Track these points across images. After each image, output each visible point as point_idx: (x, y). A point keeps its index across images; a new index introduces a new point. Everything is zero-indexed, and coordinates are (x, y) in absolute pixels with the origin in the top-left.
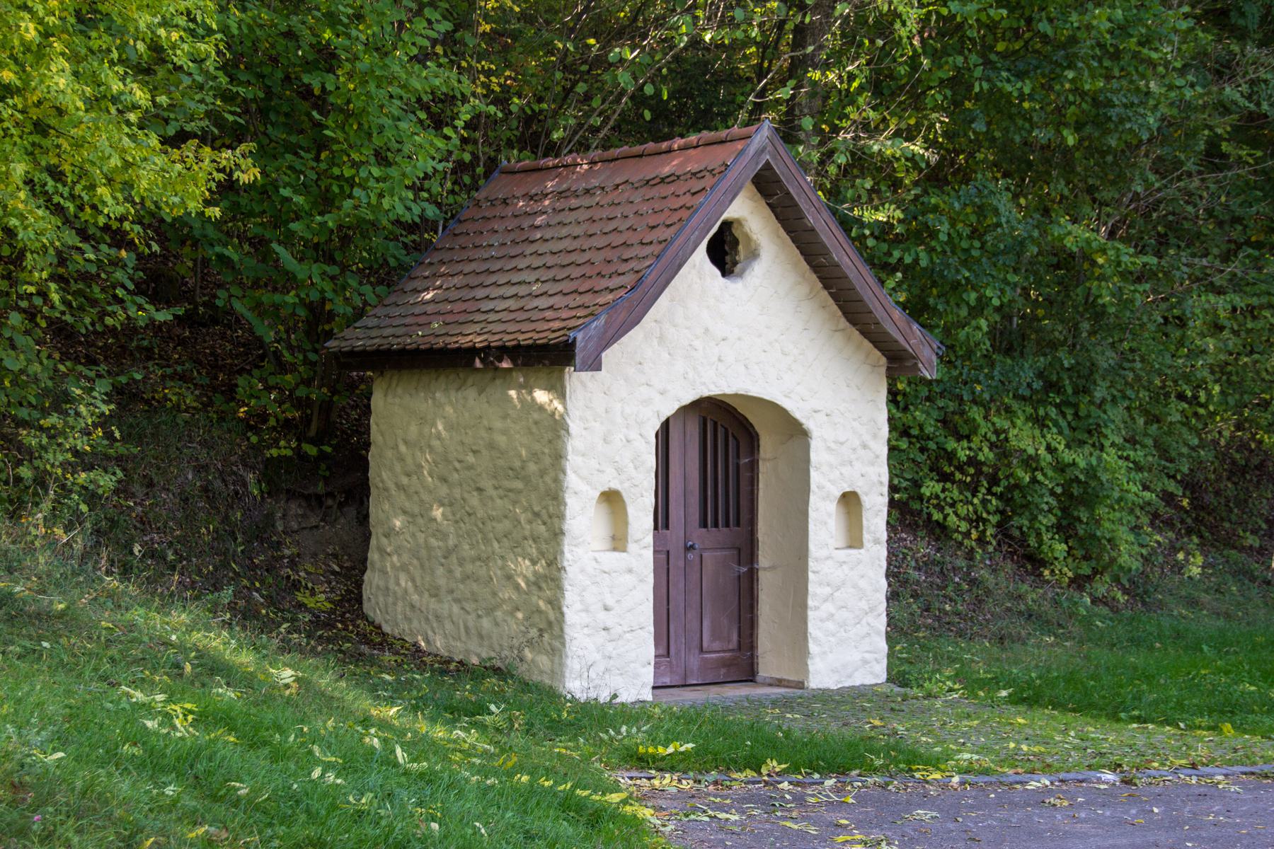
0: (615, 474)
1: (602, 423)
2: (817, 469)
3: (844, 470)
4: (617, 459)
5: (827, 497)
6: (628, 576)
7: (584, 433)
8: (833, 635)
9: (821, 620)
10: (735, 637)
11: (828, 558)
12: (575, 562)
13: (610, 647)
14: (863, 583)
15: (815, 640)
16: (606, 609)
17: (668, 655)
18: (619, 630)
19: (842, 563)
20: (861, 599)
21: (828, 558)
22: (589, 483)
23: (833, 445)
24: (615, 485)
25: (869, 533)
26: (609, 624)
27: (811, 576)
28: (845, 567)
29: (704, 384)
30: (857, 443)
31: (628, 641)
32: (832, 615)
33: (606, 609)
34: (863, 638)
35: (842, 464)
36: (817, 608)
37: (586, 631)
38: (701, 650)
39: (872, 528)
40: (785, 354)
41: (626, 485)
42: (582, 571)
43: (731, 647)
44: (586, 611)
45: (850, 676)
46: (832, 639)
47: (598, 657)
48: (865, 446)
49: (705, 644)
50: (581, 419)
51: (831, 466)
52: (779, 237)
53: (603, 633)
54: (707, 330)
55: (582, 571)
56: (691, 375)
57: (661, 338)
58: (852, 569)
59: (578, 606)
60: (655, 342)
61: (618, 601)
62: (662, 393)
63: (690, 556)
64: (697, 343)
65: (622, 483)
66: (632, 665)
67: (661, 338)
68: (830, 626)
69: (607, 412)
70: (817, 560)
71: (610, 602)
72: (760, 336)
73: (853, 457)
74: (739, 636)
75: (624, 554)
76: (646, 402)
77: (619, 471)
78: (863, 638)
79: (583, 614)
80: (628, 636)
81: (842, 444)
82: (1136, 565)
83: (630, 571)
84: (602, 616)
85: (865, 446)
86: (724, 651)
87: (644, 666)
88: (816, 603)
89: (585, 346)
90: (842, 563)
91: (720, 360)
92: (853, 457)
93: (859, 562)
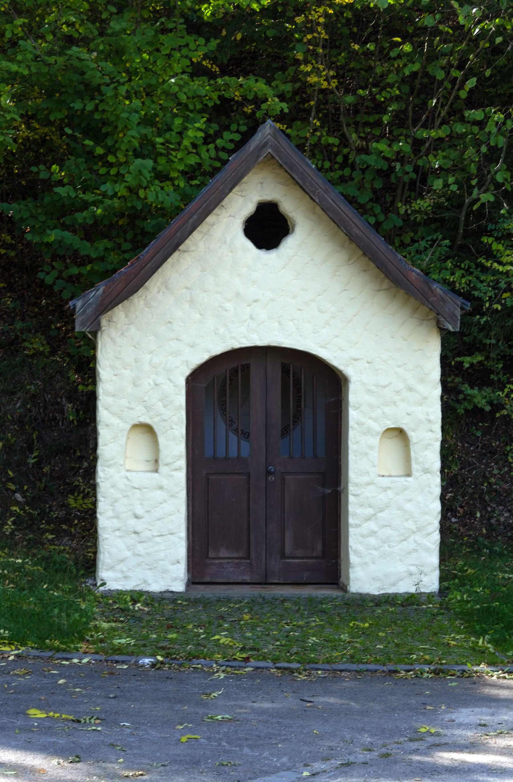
0: (145, 410)
1: (131, 370)
2: (356, 409)
3: (386, 410)
4: (146, 398)
5: (369, 432)
6: (159, 493)
7: (114, 378)
8: (376, 549)
9: (362, 536)
10: (319, 547)
11: (369, 484)
12: (107, 479)
13: (140, 548)
14: (409, 506)
15: (356, 552)
16: (137, 517)
17: (248, 557)
18: (148, 534)
19: (386, 489)
20: (407, 520)
21: (369, 484)
22: (120, 418)
23: (374, 389)
24: (145, 419)
25: (417, 463)
26: (138, 529)
27: (351, 498)
28: (389, 492)
29: (234, 338)
30: (401, 386)
31: (158, 543)
32: (375, 532)
33: (137, 517)
34: (409, 553)
35: (386, 404)
36: (358, 526)
37: (117, 533)
38: (283, 556)
39: (421, 459)
40: (321, 312)
41: (156, 419)
42: (113, 486)
43: (315, 554)
44: (117, 517)
45: (394, 585)
46: (375, 553)
47: (128, 554)
48: (410, 389)
49: (287, 551)
50: (111, 367)
51: (372, 407)
52: (314, 213)
53: (134, 536)
54: (238, 294)
55: (113, 486)
56: (222, 331)
57: (192, 302)
58: (397, 494)
59: (110, 513)
60: (187, 306)
61: (147, 512)
62: (192, 346)
63: (271, 478)
64: (229, 305)
65: (151, 418)
66: (161, 563)
67: (192, 302)
68: (372, 541)
69: (136, 361)
70: (356, 485)
71: (140, 511)
72: (295, 297)
73: (396, 398)
74: (324, 545)
75: (156, 475)
76: (177, 354)
77: (148, 408)
78: (409, 553)
79: (115, 520)
80: (158, 539)
81: (384, 387)
82: (24, 500)
83: (161, 488)
84: (133, 522)
85: (410, 389)
86: (307, 558)
87: (173, 564)
88: (358, 522)
89: (84, 311)
90: (386, 489)
91: (252, 318)
92: (396, 398)
93: (406, 489)
